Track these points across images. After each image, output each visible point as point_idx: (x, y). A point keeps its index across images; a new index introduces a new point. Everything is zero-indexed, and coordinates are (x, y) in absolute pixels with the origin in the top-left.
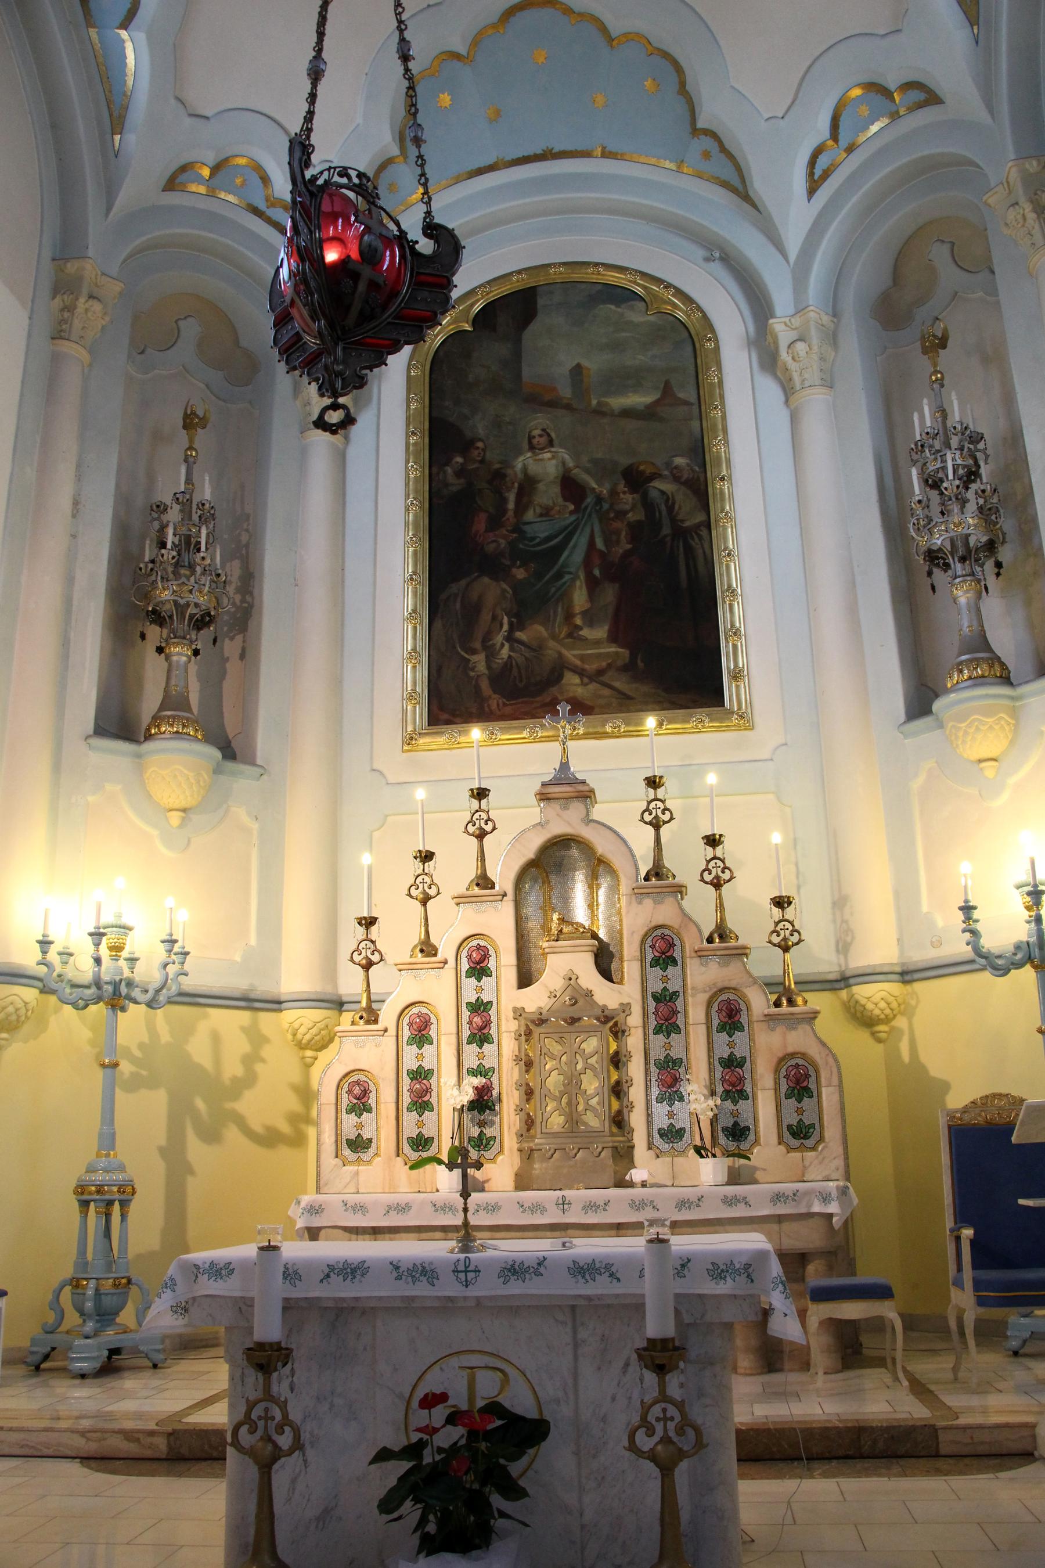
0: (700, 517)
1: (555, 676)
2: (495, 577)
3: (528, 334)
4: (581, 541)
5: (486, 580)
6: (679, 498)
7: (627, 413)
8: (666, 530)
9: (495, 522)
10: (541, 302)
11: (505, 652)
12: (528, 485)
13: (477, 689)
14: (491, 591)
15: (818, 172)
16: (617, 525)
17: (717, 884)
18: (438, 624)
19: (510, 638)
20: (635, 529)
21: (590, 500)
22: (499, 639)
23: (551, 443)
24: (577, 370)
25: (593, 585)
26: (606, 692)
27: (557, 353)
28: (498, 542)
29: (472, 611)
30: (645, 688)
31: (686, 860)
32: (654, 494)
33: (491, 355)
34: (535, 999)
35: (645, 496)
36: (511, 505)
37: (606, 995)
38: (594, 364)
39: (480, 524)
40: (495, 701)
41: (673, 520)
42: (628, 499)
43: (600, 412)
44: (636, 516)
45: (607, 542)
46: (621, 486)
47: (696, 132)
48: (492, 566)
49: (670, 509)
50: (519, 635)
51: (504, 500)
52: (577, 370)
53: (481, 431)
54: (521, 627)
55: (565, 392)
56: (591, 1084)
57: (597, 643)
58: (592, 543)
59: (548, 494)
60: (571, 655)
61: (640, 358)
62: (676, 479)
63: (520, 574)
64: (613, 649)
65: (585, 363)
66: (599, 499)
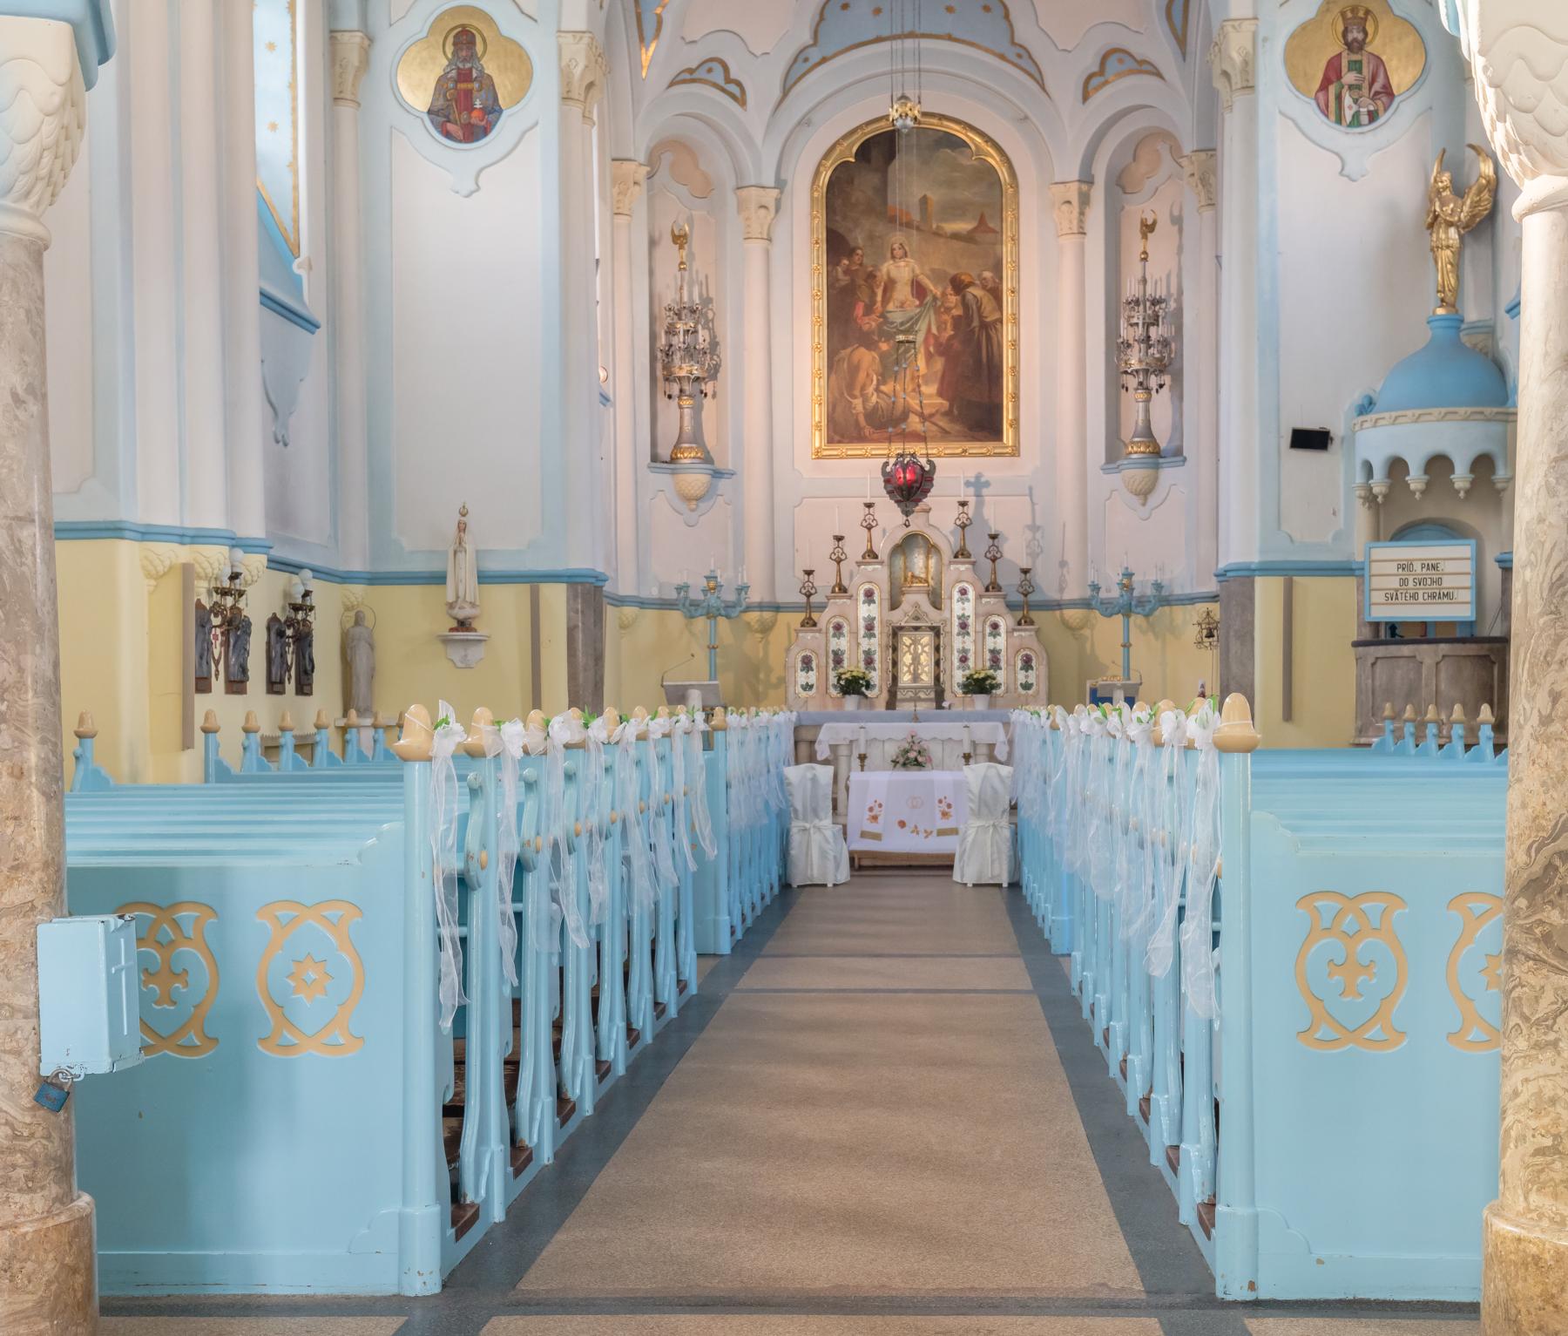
0: (997, 316)
1: (904, 416)
2: (868, 348)
3: (891, 168)
4: (922, 326)
5: (862, 350)
6: (985, 301)
7: (956, 236)
8: (976, 323)
9: (869, 310)
10: (902, 143)
11: (874, 399)
12: (890, 285)
13: (857, 421)
14: (867, 359)
15: (1090, 87)
16: (946, 317)
17: (994, 560)
18: (833, 377)
19: (877, 390)
20: (957, 322)
21: (929, 298)
22: (871, 389)
23: (906, 255)
24: (924, 201)
25: (929, 357)
26: (934, 428)
27: (911, 185)
28: (870, 323)
29: (854, 370)
30: (958, 427)
31: (979, 547)
32: (969, 297)
33: (867, 182)
34: (898, 617)
35: (964, 297)
36: (879, 298)
37: (934, 617)
38: (935, 196)
39: (859, 310)
40: (868, 431)
41: (981, 317)
42: (953, 299)
43: (938, 234)
44: (958, 312)
45: (938, 328)
46: (949, 290)
47: (1013, 43)
48: (868, 341)
49: (979, 308)
50: (883, 388)
51: (874, 294)
52: (924, 201)
53: (860, 242)
54: (885, 383)
55: (916, 216)
56: (923, 658)
57: (930, 396)
58: (929, 330)
59: (903, 292)
60: (914, 403)
61: (964, 194)
62: (984, 287)
63: (884, 347)
64: (940, 401)
65: (929, 194)
66: (935, 298)
